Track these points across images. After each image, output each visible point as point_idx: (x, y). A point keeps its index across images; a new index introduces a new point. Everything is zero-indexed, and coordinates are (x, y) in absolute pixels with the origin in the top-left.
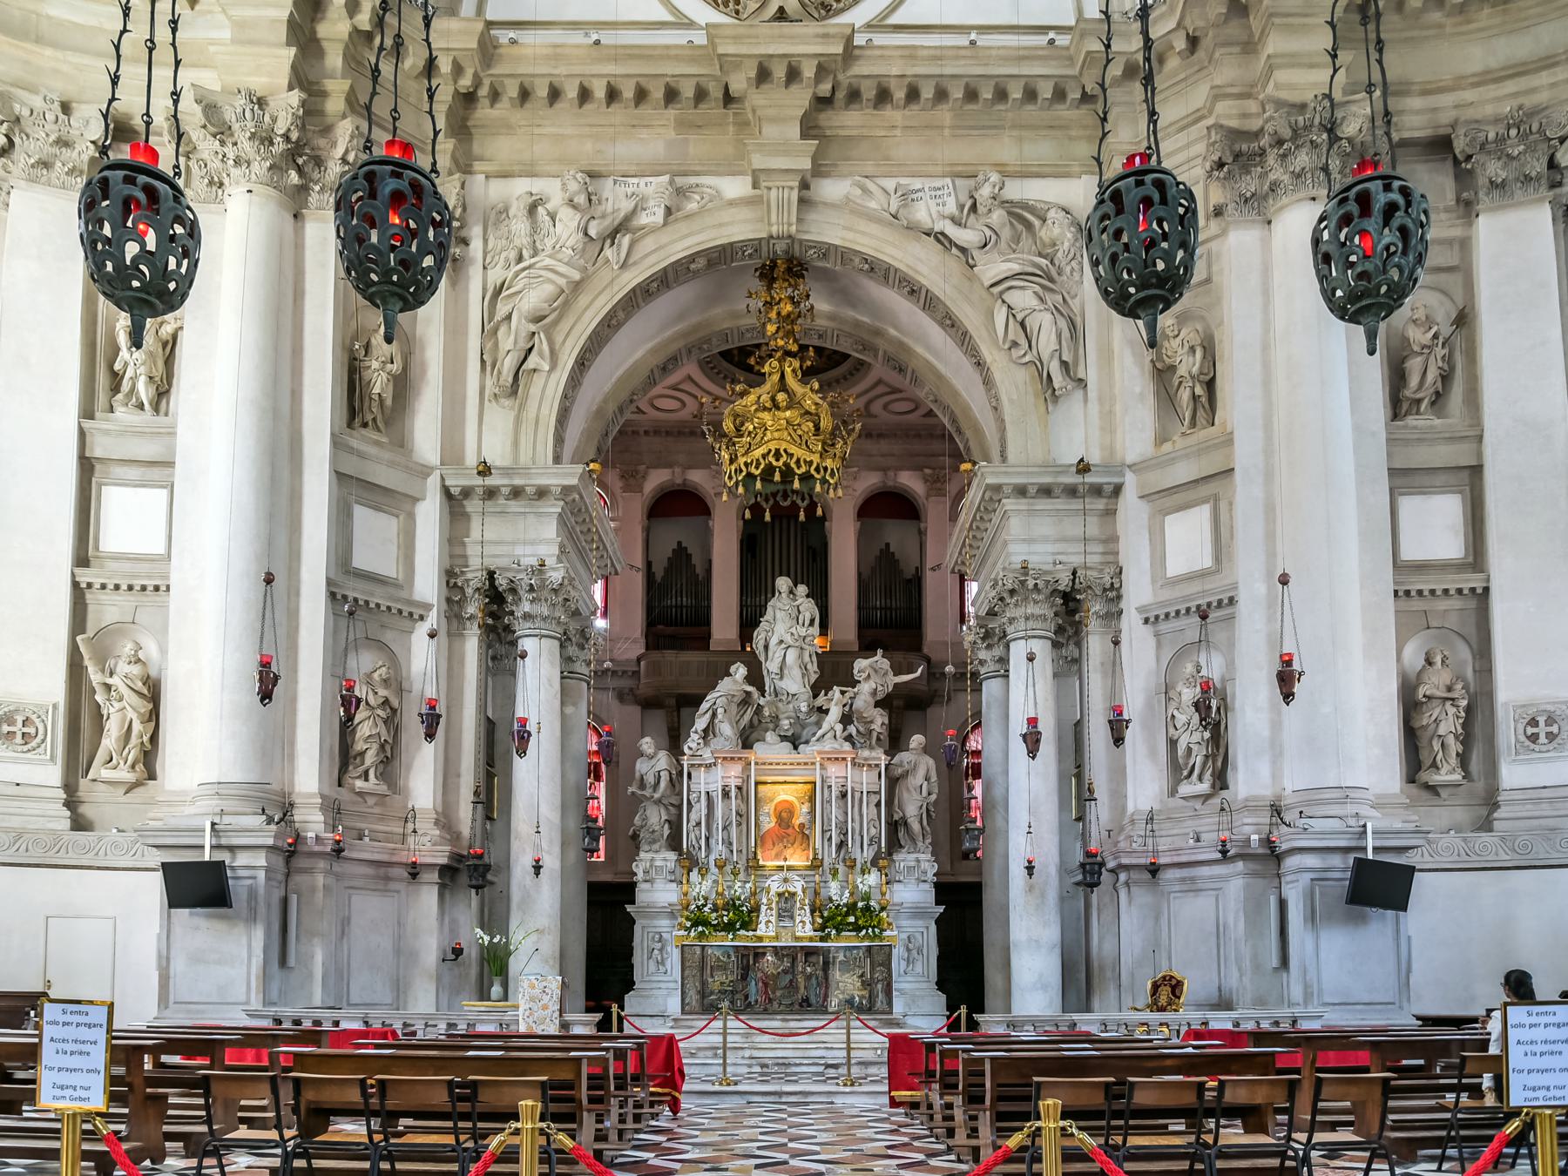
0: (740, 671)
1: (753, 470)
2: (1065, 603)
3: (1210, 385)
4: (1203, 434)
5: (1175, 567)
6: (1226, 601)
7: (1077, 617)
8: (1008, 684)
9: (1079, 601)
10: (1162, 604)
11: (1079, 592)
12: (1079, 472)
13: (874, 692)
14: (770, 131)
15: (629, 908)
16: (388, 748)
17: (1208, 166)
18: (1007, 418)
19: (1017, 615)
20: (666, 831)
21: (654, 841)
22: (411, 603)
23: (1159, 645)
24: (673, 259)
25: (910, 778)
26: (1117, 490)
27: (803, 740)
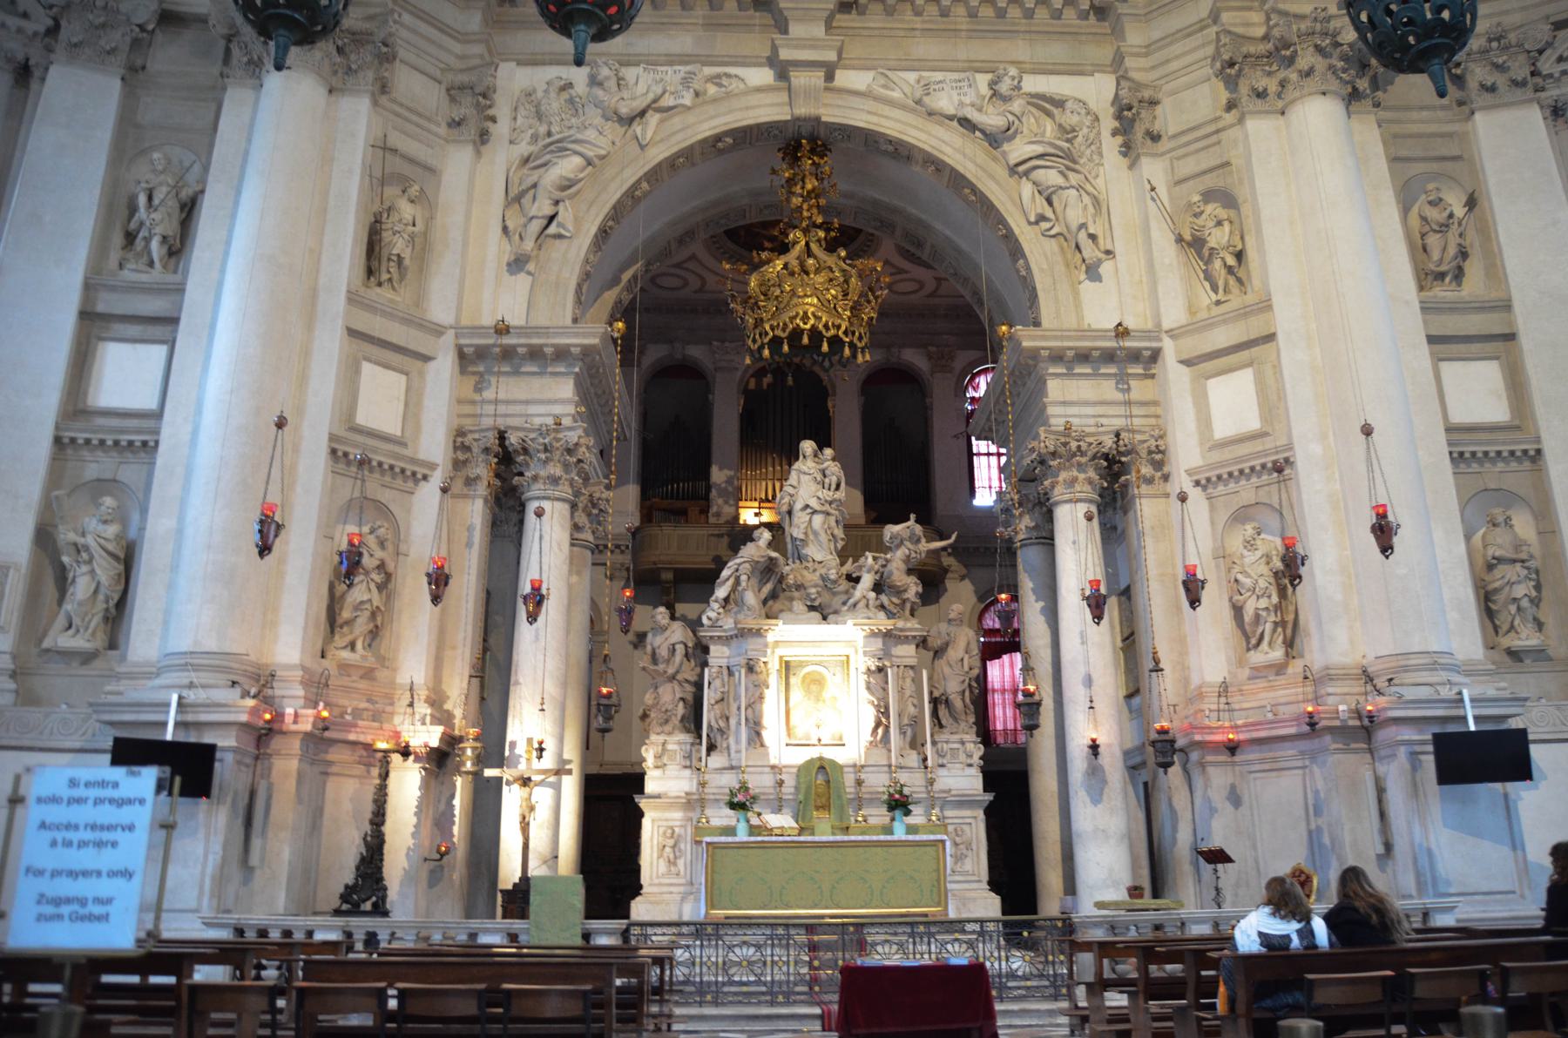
1: (779, 333)
2: (1109, 467)
3: (1239, 256)
4: (1236, 300)
5: (1223, 428)
10: (1211, 467)
12: (1117, 336)
13: (907, 559)
14: (796, 30)
15: (637, 798)
17: (1218, 65)
20: (681, 710)
21: (667, 721)
22: (413, 461)
23: (1212, 509)
24: (700, 137)
26: (1155, 355)
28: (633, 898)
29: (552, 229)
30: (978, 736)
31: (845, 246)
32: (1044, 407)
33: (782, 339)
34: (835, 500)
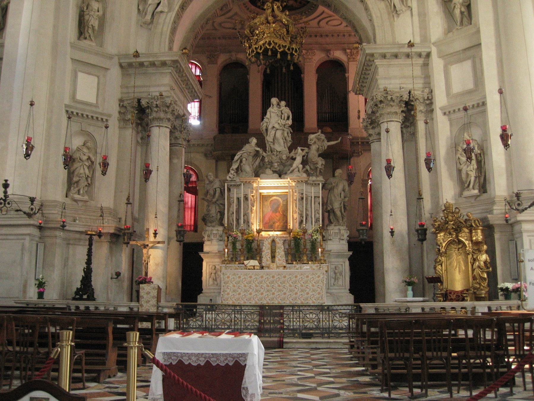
0: (254, 141)
1: (259, 50)
5: (456, 88)
6: (481, 104)
7: (412, 113)
8: (381, 143)
9: (413, 105)
11: (412, 101)
13: (318, 150)
16: (89, 179)
18: (376, 24)
19: (383, 112)
20: (219, 217)
21: (213, 222)
22: (101, 114)
23: (451, 125)
25: (335, 190)
26: (428, 55)
27: (284, 172)
28: (199, 294)
29: (159, 9)
30: (347, 227)
31: (289, 11)
32: (377, 80)
33: (260, 53)
34: (287, 124)
